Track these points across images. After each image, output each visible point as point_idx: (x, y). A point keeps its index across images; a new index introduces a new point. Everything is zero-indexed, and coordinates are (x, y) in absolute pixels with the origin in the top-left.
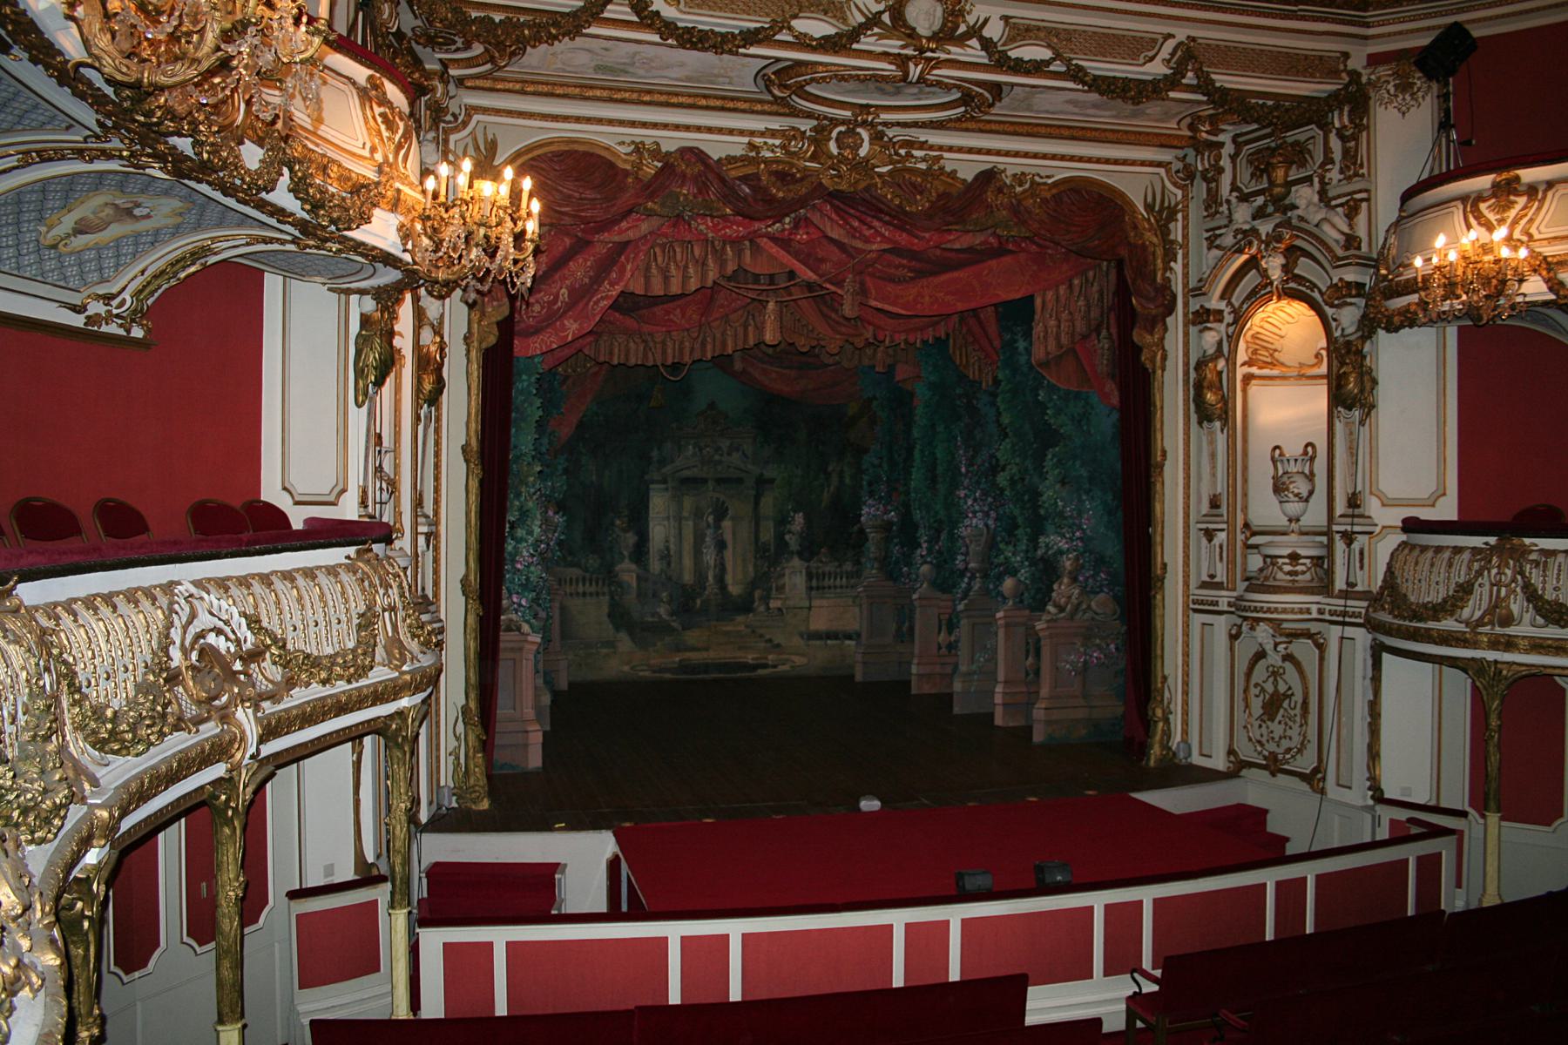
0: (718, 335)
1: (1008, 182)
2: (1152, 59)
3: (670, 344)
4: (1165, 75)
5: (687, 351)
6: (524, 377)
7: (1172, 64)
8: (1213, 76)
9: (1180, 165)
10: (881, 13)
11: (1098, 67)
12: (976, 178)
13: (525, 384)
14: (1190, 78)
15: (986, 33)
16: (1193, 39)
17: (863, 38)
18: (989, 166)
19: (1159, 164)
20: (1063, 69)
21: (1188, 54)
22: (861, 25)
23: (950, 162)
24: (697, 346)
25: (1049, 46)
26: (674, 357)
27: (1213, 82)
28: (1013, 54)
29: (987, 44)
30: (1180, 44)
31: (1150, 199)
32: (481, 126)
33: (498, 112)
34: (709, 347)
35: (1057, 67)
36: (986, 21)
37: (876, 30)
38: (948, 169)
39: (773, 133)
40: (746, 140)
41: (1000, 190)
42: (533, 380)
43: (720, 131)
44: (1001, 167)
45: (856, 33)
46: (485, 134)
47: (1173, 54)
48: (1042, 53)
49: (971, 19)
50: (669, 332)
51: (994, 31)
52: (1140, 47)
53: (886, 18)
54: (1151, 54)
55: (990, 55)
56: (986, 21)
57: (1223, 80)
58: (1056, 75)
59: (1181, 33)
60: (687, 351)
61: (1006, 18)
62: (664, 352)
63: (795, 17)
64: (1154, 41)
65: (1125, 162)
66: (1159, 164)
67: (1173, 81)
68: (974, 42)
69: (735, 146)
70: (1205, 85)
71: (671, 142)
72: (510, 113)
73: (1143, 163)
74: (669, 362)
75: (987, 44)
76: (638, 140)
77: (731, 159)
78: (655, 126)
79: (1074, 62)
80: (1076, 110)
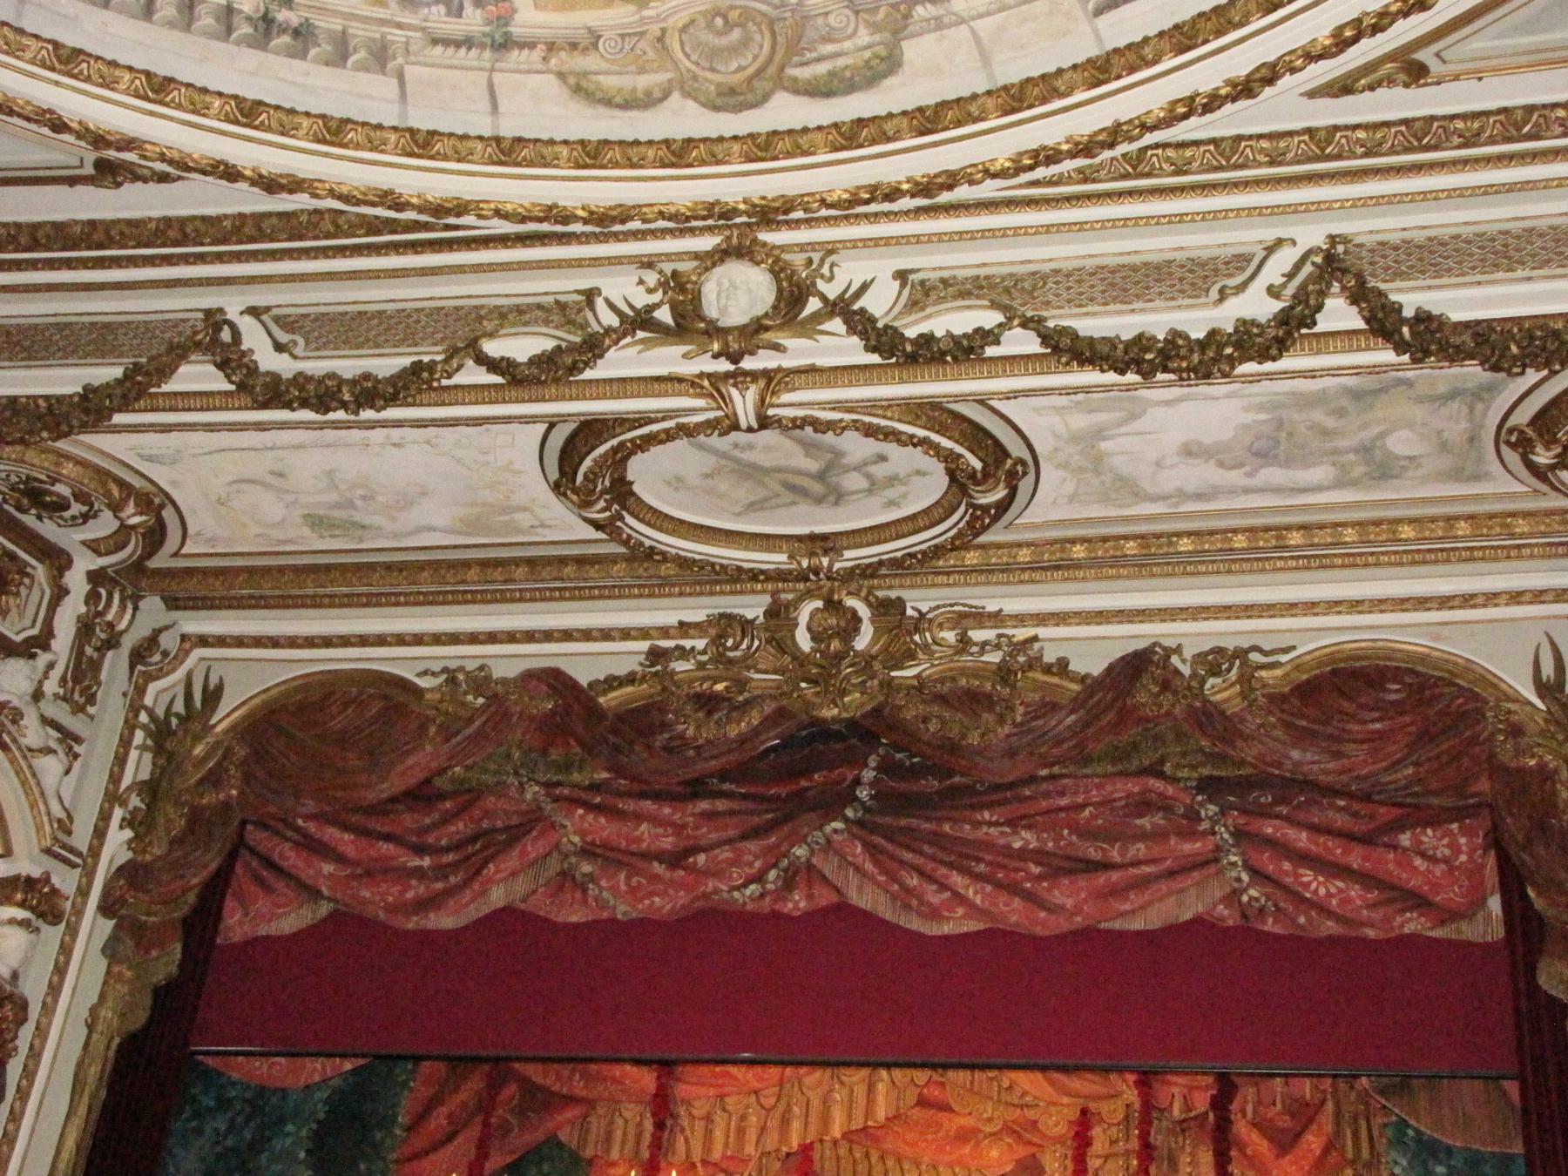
0: (816, 1103)
1: (1186, 670)
2: (1242, 287)
3: (720, 1119)
5: (752, 1135)
6: (290, 1128)
7: (1290, 291)
11: (1094, 324)
12: (1110, 669)
13: (289, 1141)
14: (1338, 314)
18: (1141, 645)
22: (609, 331)
23: (1054, 642)
24: (773, 1123)
25: (994, 305)
26: (726, 1145)
29: (860, 324)
31: (1548, 670)
32: (204, 666)
33: (240, 642)
34: (796, 1125)
36: (865, 287)
37: (640, 334)
38: (1050, 657)
39: (684, 628)
40: (644, 646)
41: (1165, 686)
42: (304, 1133)
43: (587, 635)
44: (1171, 643)
45: (593, 347)
46: (207, 676)
47: (1290, 276)
49: (832, 291)
50: (722, 1097)
51: (879, 303)
53: (664, 315)
56: (865, 287)
60: (752, 1135)
61: (902, 276)
62: (708, 1134)
63: (491, 335)
64: (1245, 259)
65: (1467, 600)
68: (837, 325)
69: (627, 657)
71: (508, 662)
72: (258, 642)
74: (716, 1155)
75: (860, 324)
76: (453, 665)
77: (612, 682)
78: (474, 638)
79: (1051, 324)
80: (1236, 477)
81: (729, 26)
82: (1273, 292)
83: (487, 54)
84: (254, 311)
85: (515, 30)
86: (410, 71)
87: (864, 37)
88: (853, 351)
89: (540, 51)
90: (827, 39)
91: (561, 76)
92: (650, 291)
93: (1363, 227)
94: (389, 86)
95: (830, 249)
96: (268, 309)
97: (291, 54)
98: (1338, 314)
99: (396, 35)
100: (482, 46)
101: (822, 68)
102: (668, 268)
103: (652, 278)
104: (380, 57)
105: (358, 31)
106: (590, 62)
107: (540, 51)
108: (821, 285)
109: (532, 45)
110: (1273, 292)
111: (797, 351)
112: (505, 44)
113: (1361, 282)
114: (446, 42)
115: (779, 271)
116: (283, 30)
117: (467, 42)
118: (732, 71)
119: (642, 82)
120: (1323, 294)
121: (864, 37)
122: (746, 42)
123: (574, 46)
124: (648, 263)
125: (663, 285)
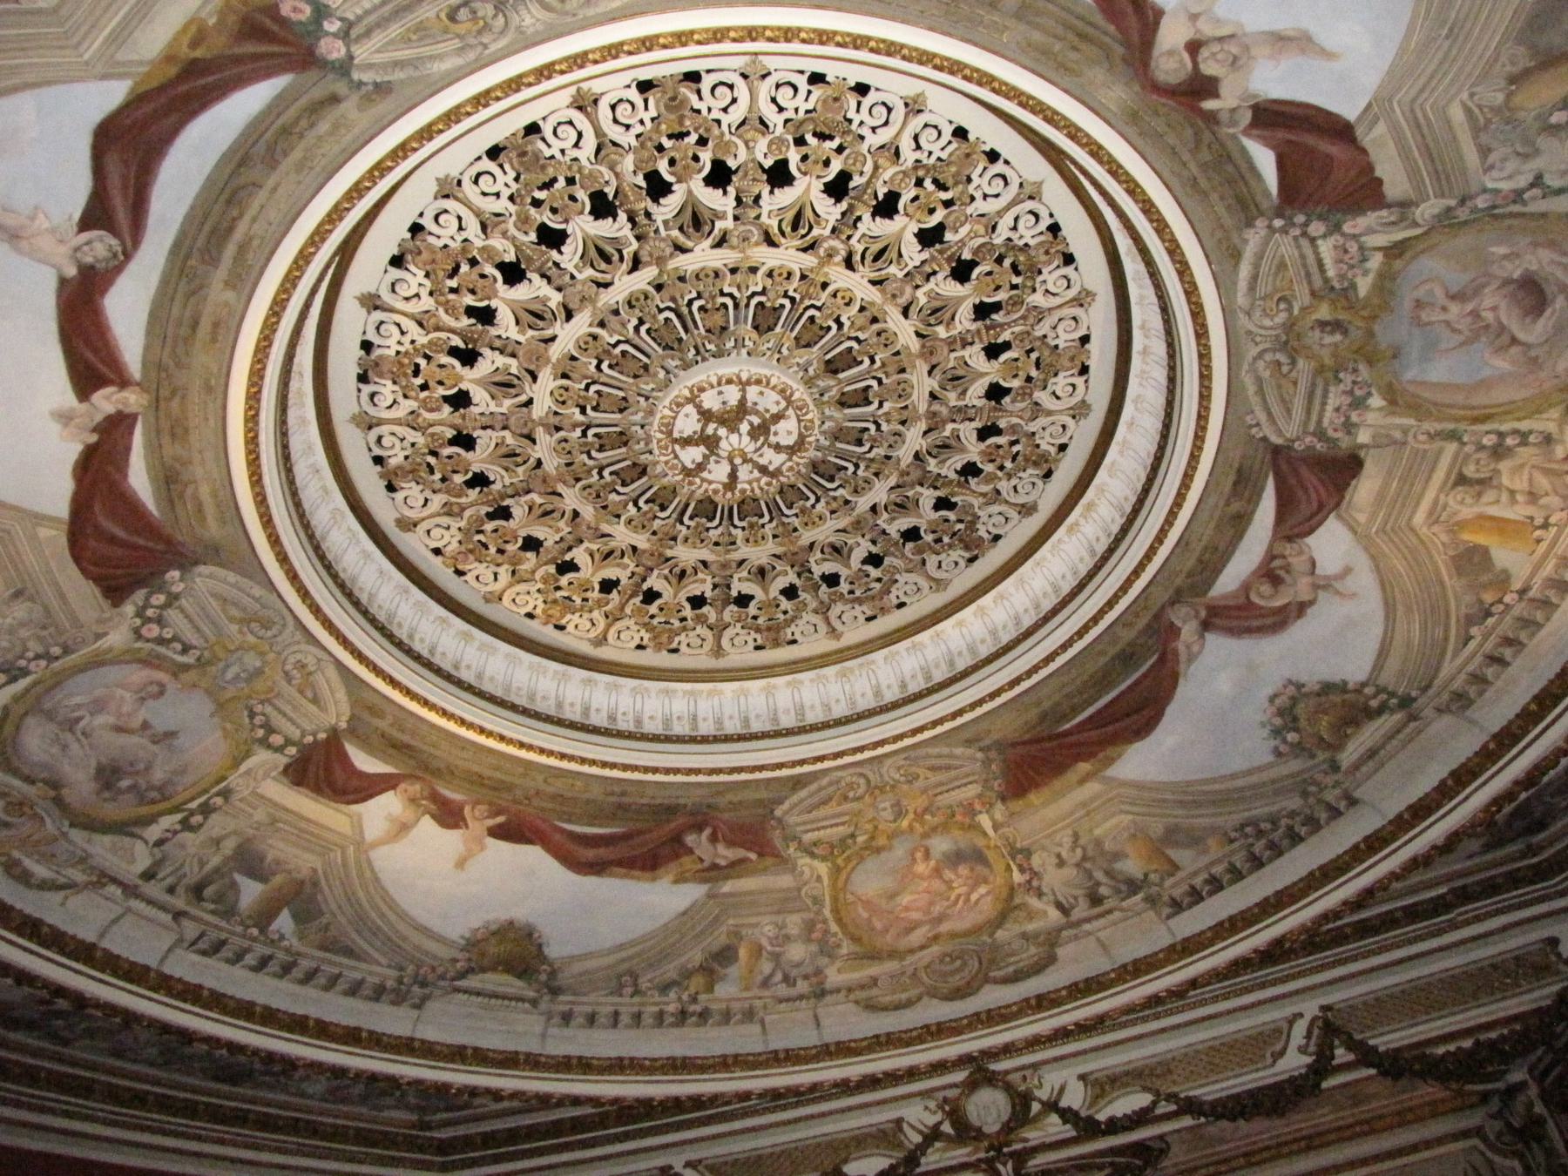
2: (1282, 1053)
4: (1308, 1066)
7: (1312, 1049)
8: (1371, 1042)
9: (1498, 1125)
10: (940, 1123)
11: (1210, 1091)
14: (1341, 1055)
15: (1063, 1104)
16: (1326, 1008)
17: (923, 1160)
19: (1465, 1134)
20: (1173, 1107)
21: (1329, 1028)
22: (918, 1146)
25: (1145, 1089)
27: (1374, 1049)
28: (1102, 1117)
29: (1067, 1115)
30: (1314, 1020)
35: (1164, 1108)
36: (1062, 1089)
47: (1308, 1036)
48: (1141, 1100)
49: (1043, 1094)
51: (1075, 1098)
52: (1268, 1042)
53: (947, 1128)
54: (1278, 1047)
55: (1076, 1125)
56: (1062, 1089)
57: (1387, 1040)
58: (1168, 1117)
59: (1310, 1008)
61: (1082, 1077)
63: (846, 1161)
64: (1278, 1031)
66: (1465, 1134)
67: (1322, 1066)
68: (1054, 1118)
70: (1366, 1055)
73: (1440, 1141)
75: (1067, 1115)
79: (1182, 1095)
81: (953, 960)
82: (1302, 1050)
83: (813, 1000)
84: (688, 1164)
85: (828, 986)
86: (768, 1019)
87: (1033, 950)
88: (1069, 1131)
89: (843, 993)
90: (1013, 955)
91: (857, 1002)
92: (935, 1113)
93: (1334, 997)
94: (756, 1028)
95: (1035, 1066)
96: (700, 1161)
97: (698, 1025)
98: (1341, 1055)
99: (758, 1003)
100: (808, 998)
101: (1011, 969)
102: (940, 1095)
103: (932, 1105)
104: (749, 1015)
105: (736, 1006)
106: (875, 992)
107: (843, 993)
108: (1037, 1093)
109: (838, 991)
110: (1302, 1050)
111: (1033, 1135)
112: (821, 993)
113: (1350, 1036)
114: (788, 1000)
115: (1008, 1088)
116: (693, 1014)
117: (801, 997)
118: (956, 981)
119: (904, 996)
120: (1332, 1048)
121: (1033, 950)
122: (965, 964)
123: (862, 987)
124: (926, 1094)
125: (941, 1107)
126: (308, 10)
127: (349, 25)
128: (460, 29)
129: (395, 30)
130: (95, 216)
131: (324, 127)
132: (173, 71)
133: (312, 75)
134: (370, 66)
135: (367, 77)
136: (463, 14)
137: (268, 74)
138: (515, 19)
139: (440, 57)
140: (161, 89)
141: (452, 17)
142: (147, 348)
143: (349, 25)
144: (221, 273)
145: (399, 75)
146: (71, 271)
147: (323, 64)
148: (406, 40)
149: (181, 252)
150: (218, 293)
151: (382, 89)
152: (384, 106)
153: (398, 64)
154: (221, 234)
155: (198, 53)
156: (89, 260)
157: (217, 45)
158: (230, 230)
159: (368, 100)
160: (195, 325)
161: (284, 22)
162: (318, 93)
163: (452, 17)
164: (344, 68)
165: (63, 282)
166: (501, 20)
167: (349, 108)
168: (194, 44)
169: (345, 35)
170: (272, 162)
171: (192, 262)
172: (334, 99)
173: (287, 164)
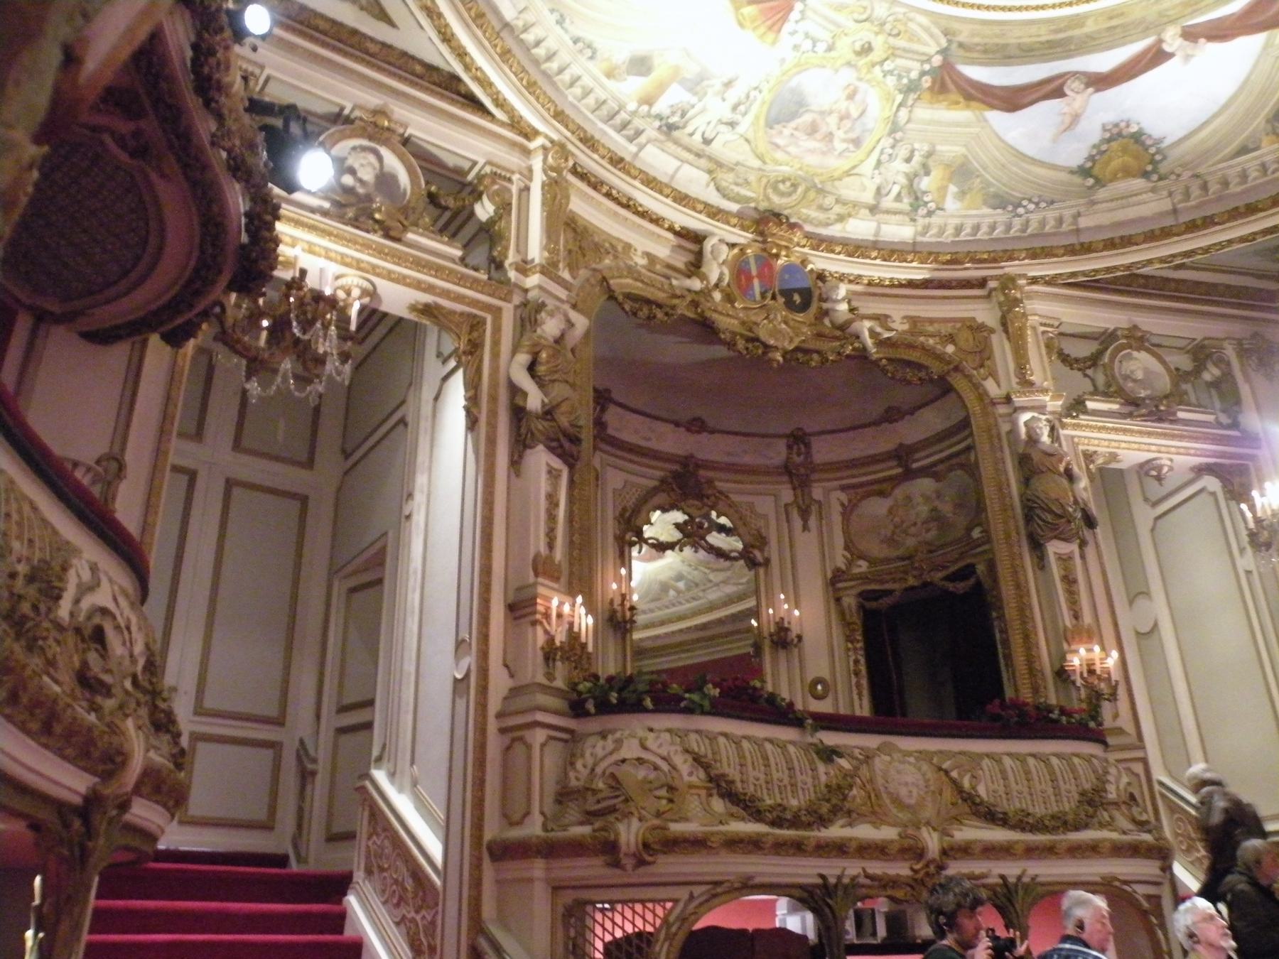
126: (924, 78)
127: (923, 62)
128: (902, 28)
129: (916, 47)
130: (1059, 93)
131: (977, 40)
132: (973, 104)
133: (952, 60)
134: (938, 44)
135: (944, 43)
136: (895, 32)
137: (961, 75)
138: (888, 13)
139: (921, 26)
140: (984, 102)
141: (898, 34)
142: (1131, 42)
143: (923, 62)
144: (1076, 32)
145: (936, 31)
146: (1091, 90)
147: (945, 59)
148: (919, 41)
149: (1068, 54)
150: (1090, 27)
151: (946, 33)
152: (956, 26)
153: (932, 36)
154: (1051, 45)
155: (961, 100)
156: (1082, 86)
157: (955, 96)
158: (1048, 42)
159: (954, 34)
160: (1114, 28)
161: (934, 82)
162: (961, 52)
163: (898, 34)
164: (944, 52)
165: (1098, 90)
166: (890, 19)
167: (961, 38)
168: (957, 103)
169: (928, 61)
170: (1005, 46)
171: (1073, 47)
172: (961, 45)
173: (1001, 41)
